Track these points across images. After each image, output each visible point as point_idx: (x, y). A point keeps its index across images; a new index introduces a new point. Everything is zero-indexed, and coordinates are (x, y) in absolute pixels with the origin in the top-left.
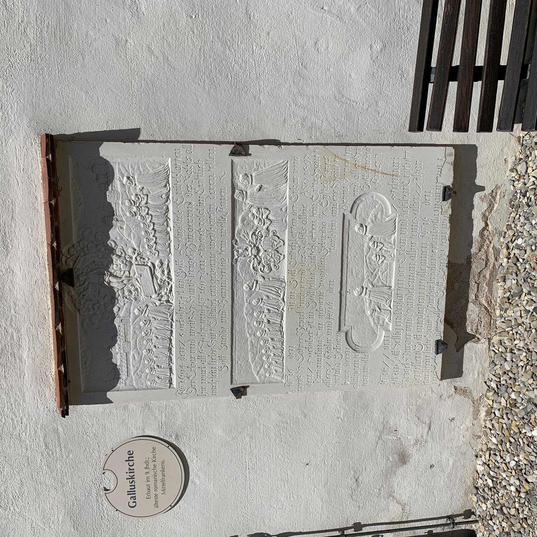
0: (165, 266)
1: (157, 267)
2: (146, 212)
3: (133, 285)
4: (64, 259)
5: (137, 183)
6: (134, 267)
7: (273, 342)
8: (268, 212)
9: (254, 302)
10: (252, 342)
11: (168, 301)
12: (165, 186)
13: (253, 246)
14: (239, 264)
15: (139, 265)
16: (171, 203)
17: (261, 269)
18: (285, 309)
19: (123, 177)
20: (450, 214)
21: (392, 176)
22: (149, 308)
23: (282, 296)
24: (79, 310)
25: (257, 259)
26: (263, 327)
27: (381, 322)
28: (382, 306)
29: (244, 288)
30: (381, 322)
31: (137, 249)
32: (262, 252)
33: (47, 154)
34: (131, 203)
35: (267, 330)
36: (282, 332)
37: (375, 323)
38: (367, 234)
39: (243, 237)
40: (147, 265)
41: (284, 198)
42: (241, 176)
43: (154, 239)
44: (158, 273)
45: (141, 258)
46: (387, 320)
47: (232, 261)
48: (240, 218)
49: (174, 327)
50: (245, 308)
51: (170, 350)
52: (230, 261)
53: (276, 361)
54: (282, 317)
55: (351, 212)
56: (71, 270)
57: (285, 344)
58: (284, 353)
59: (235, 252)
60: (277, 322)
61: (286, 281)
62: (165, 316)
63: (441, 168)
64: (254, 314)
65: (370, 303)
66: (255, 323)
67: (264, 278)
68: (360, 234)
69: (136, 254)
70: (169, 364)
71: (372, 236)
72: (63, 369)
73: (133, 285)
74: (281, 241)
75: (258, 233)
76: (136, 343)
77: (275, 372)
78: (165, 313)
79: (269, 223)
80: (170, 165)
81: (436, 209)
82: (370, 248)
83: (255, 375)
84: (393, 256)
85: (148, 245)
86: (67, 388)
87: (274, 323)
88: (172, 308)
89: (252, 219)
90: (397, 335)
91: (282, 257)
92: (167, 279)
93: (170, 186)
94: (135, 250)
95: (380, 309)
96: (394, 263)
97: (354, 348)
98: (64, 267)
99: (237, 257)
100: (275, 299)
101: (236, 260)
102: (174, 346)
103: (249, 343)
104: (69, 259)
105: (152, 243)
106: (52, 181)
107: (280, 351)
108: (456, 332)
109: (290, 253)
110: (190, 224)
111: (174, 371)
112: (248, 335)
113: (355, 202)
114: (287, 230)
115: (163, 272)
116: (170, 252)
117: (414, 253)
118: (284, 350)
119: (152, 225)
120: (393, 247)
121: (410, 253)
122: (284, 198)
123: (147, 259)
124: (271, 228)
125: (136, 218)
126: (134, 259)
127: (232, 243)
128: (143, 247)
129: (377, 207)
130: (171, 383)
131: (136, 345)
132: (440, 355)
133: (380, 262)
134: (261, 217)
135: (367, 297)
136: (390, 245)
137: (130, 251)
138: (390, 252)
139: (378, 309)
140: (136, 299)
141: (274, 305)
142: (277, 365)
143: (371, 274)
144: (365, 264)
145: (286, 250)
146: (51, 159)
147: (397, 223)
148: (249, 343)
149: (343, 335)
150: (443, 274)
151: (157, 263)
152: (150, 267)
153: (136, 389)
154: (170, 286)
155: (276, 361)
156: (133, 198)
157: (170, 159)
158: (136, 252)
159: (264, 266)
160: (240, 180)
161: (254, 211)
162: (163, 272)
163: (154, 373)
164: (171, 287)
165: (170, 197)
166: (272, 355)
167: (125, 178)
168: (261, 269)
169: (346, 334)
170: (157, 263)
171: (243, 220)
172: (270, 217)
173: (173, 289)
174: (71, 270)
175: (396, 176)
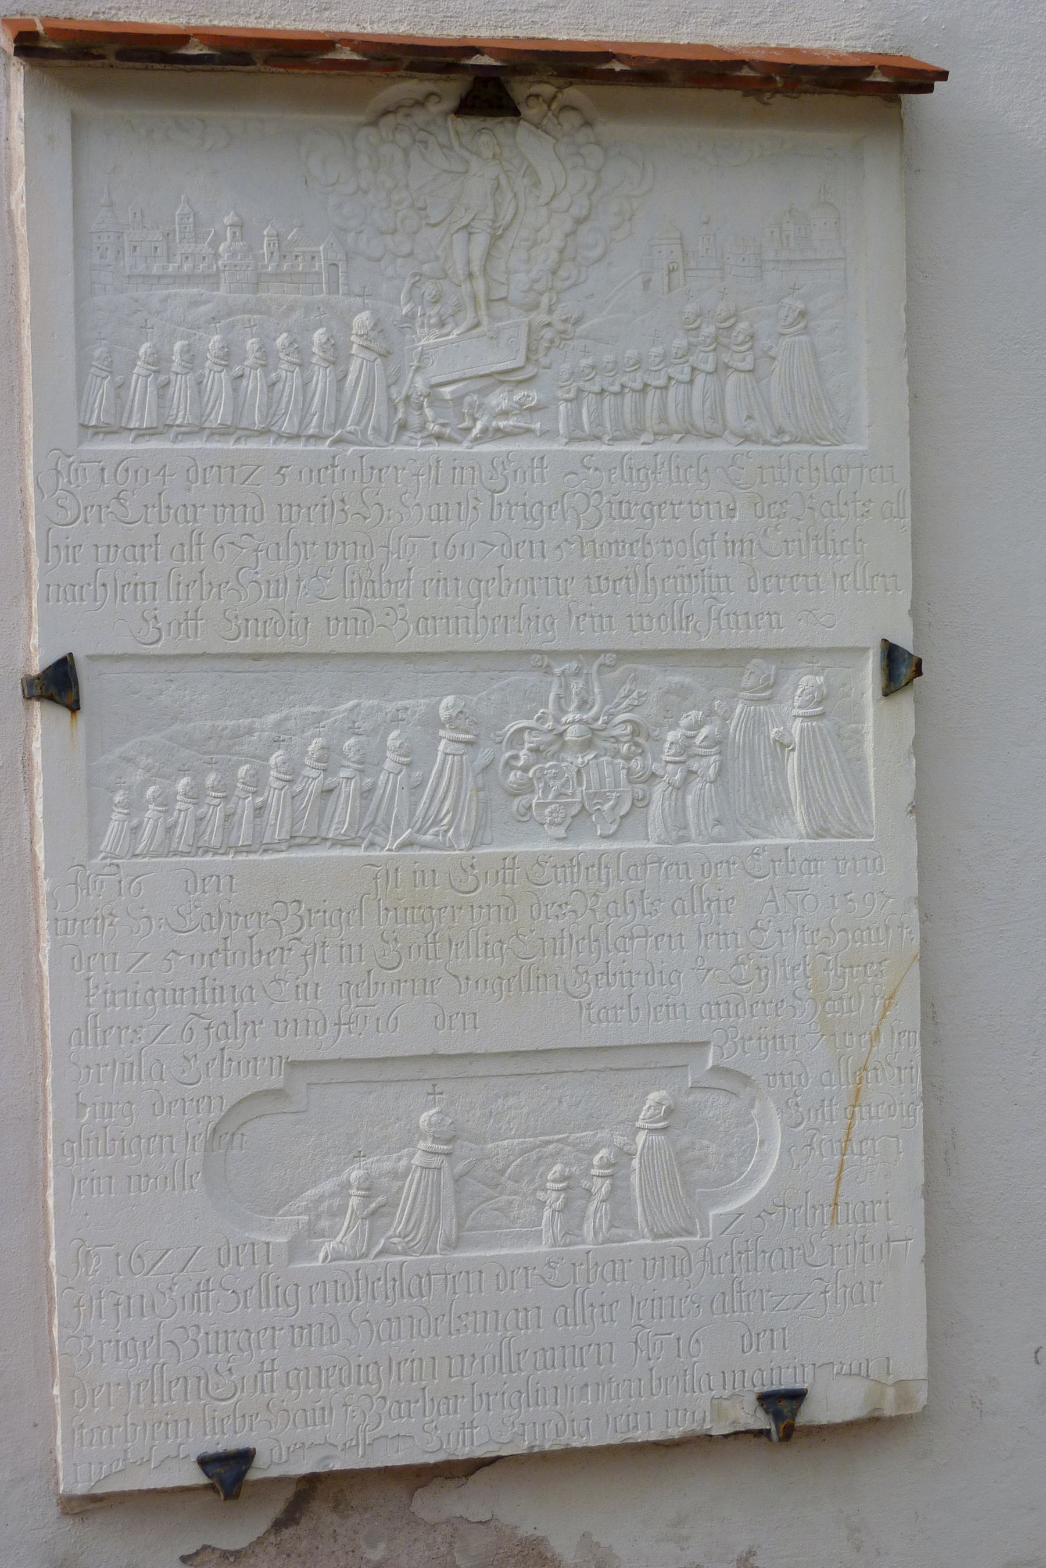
2: (702, 366)
4: (547, 90)
10: (250, 731)
11: (403, 427)
12: (781, 432)
13: (596, 726)
15: (530, 332)
16: (731, 448)
18: (375, 853)
24: (374, 123)
25: (551, 744)
28: (385, 1220)
31: (580, 329)
33: (885, 69)
34: (727, 319)
35: (297, 788)
36: (292, 842)
37: (321, 1199)
39: (623, 692)
40: (528, 359)
41: (754, 831)
42: (820, 680)
43: (616, 388)
44: (499, 399)
45: (552, 341)
47: (541, 652)
48: (687, 680)
52: (545, 647)
54: (343, 844)
56: (516, 113)
57: (241, 858)
58: (208, 858)
59: (574, 665)
60: (324, 826)
61: (474, 852)
63: (863, 1372)
67: (486, 768)
68: (639, 1111)
69: (560, 327)
70: (170, 426)
72: (195, 52)
73: (459, 308)
74: (614, 827)
76: (251, 312)
81: (729, 1377)
82: (593, 1151)
86: (113, 60)
94: (577, 322)
95: (373, 1213)
98: (519, 89)
100: (412, 814)
101: (548, 670)
102: (242, 446)
104: (545, 107)
106: (804, 78)
108: (260, 1541)
110: (666, 510)
112: (272, 718)
115: (505, 414)
117: (579, 1320)
118: (218, 858)
120: (600, 1237)
121: (578, 1305)
122: (754, 831)
123: (545, 361)
126: (544, 318)
127: (606, 652)
132: (199, 1478)
141: (389, 813)
142: (160, 831)
143: (500, 1166)
146: (871, 79)
147: (678, 1239)
149: (276, 1081)
150: (505, 1438)
152: (522, 368)
154: (456, 436)
156: (742, 326)
157: (865, 448)
159: (525, 769)
162: (505, 414)
164: (451, 440)
165: (746, 447)
167: (800, 305)
171: (683, 692)
174: (516, 113)
175: (834, 1215)
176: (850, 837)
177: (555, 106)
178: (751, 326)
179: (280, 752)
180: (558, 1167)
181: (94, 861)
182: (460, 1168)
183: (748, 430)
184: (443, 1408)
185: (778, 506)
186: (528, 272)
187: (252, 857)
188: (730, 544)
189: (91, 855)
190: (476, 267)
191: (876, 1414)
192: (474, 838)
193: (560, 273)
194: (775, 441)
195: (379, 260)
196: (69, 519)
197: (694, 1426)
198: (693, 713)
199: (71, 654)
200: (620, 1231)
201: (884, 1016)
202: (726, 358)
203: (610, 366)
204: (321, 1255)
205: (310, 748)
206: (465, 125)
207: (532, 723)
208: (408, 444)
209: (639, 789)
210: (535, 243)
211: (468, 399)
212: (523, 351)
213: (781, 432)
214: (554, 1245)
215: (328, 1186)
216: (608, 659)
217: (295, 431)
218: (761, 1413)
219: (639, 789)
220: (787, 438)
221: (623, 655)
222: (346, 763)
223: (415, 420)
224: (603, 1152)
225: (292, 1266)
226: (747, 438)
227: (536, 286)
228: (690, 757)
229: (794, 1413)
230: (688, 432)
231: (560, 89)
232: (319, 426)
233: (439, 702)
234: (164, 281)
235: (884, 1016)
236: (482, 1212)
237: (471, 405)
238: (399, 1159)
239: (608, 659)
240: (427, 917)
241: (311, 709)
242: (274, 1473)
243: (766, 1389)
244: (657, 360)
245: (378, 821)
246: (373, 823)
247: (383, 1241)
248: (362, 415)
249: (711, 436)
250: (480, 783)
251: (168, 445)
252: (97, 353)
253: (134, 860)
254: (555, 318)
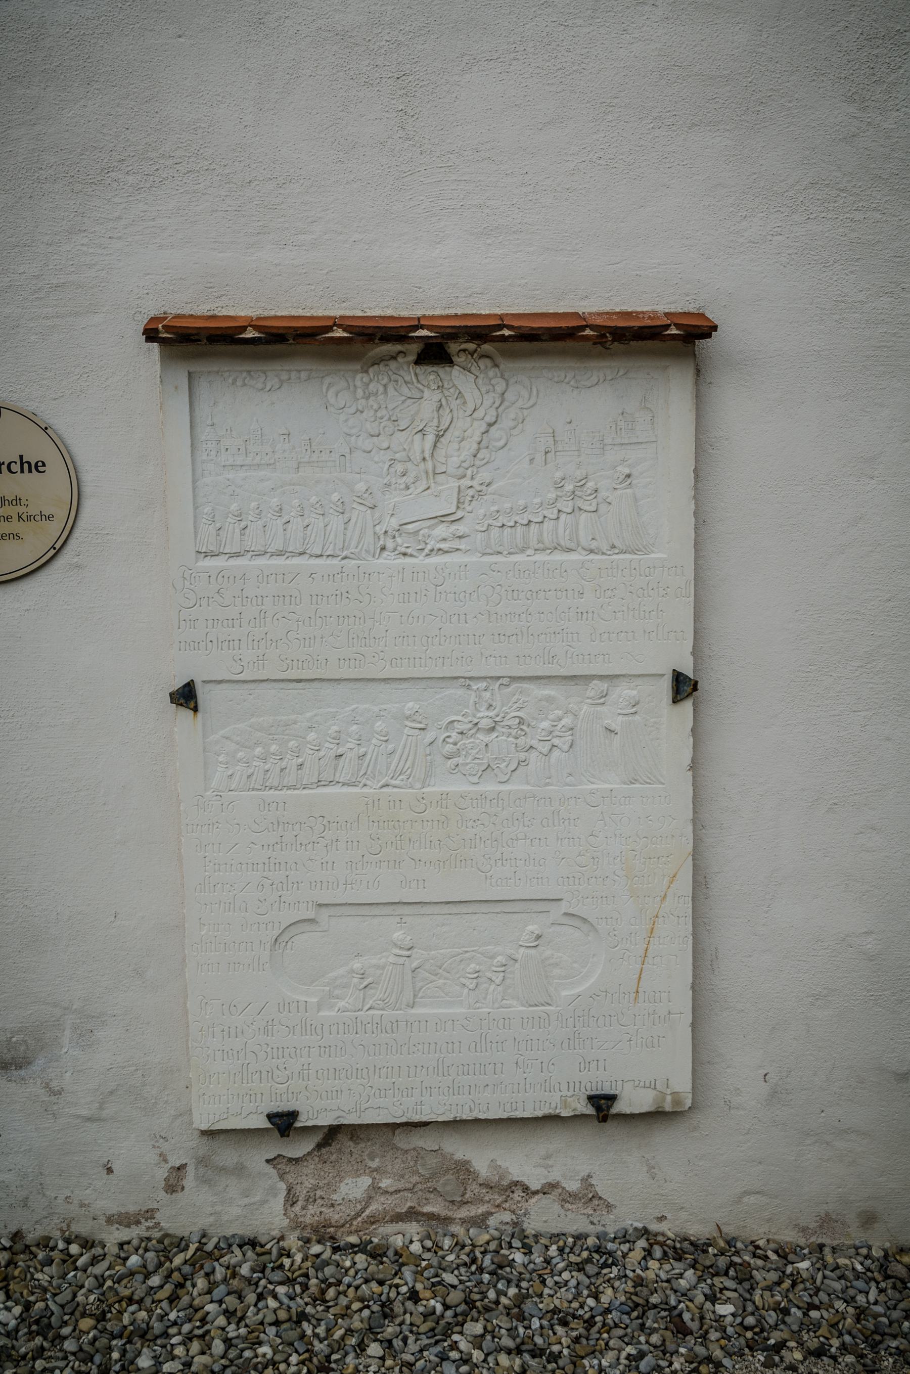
0: (456, 544)
1: (454, 527)
2: (564, 509)
3: (417, 479)
5: (619, 492)
6: (454, 484)
7: (294, 768)
8: (566, 747)
9: (379, 725)
10: (295, 723)
11: (383, 549)
13: (497, 719)
14: (461, 692)
15: (459, 491)
16: (581, 557)
17: (449, 737)
18: (365, 790)
19: (629, 466)
20: (562, 1115)
21: (635, 990)
22: (369, 511)
23: (393, 782)
26: (327, 745)
27: (337, 992)
28: (373, 991)
29: (410, 704)
30: (337, 992)
31: (491, 489)
32: (486, 738)
34: (581, 481)
35: (322, 753)
36: (319, 783)
38: (522, 950)
39: (514, 699)
40: (458, 507)
41: (592, 780)
42: (635, 692)
43: (512, 524)
44: (441, 530)
45: (473, 497)
46: (342, 1004)
48: (553, 693)
49: (330, 561)
50: (367, 706)
51: (280, 554)
52: (466, 675)
53: (252, 774)
54: (348, 785)
55: (566, 914)
57: (289, 792)
58: (272, 792)
59: (485, 684)
60: (337, 775)
61: (424, 790)
62: (354, 543)
64: (355, 727)
65: (377, 967)
66: (335, 728)
69: (479, 488)
71: (516, 961)
73: (417, 479)
74: (507, 777)
75: (522, 730)
76: (294, 484)
77: (230, 773)
78: (359, 543)
79: (545, 750)
80: (653, 555)
81: (572, 1085)
82: (492, 957)
83: (221, 733)
84: (478, 1005)
85: (498, 512)
87: (335, 769)
88: (370, 558)
89: (551, 717)
90: (309, 1027)
91: (475, 779)
92: (429, 547)
93: (615, 557)
96: (464, 1010)
97: (280, 940)
98: (453, 347)
99: (475, 688)
100: (388, 768)
101: (469, 687)
102: (288, 562)
103: (293, 717)
105: (502, 520)
107: (275, 784)
108: (309, 1154)
109: (483, 796)
111: (233, 562)
112: (309, 715)
113: (585, 920)
114: (529, 788)
116: (484, 554)
117: (484, 1050)
118: (277, 792)
119: (540, 519)
120: (496, 1005)
121: (483, 1042)
123: (469, 508)
124: (533, 755)
125: (552, 489)
126: (470, 483)
128: (493, 503)
129: (575, 965)
130: (206, 555)
131: (290, 484)
132: (267, 1125)
133: (463, 980)
134: (554, 734)
135: (392, 959)
136: (500, 998)
137: (484, 475)
138: (485, 998)
139: (365, 983)
140: (388, 485)
142: (245, 777)
144: (460, 951)
145: (489, 787)
148: (293, 717)
149: (310, 914)
151: (461, 528)
153: (194, 481)
154: (415, 554)
155: (252, 774)
156: (590, 484)
157: (665, 556)
158: (484, 488)
159: (455, 744)
161: (567, 721)
163: (229, 520)
165: (592, 556)
166: (267, 767)
167: (627, 471)
168: (449, 737)
169: (311, 921)
170: (461, 528)
171: (549, 699)
172: (556, 753)
173: (408, 560)
177: (475, 355)
178: (596, 484)
179: (313, 734)
180: (473, 966)
181: (208, 793)
182: (414, 965)
183: (592, 547)
184: (405, 1094)
185: (609, 592)
186: (459, 456)
187: (296, 792)
188: (580, 614)
189: (206, 791)
190: (427, 455)
191: (660, 1110)
192: (424, 782)
193: (478, 456)
194: (609, 553)
195: (370, 452)
196: (191, 605)
197: (550, 1111)
198: (556, 712)
199: (192, 681)
200: (508, 1002)
201: (669, 887)
202: (579, 503)
203: (508, 511)
204: (336, 1009)
205: (330, 732)
206: (419, 370)
207: (459, 718)
208: (386, 559)
209: (522, 756)
210: (463, 439)
211: (422, 532)
212: (455, 503)
213: (613, 547)
214: (469, 1008)
215: (341, 971)
216: (505, 681)
217: (319, 553)
218: (589, 1106)
219: (522, 756)
220: (617, 551)
221: (514, 679)
222: (350, 740)
223: (390, 544)
224: (499, 958)
225: (320, 1014)
226: (592, 551)
227: (464, 465)
228: (553, 737)
229: (609, 1107)
230: (556, 548)
231: (479, 345)
232: (334, 550)
233: (404, 706)
234: (244, 468)
235: (669, 887)
236: (428, 988)
237: (424, 536)
238: (380, 959)
239: (505, 681)
240: (396, 826)
241: (332, 710)
242: (310, 1123)
243: (593, 1093)
244: (537, 506)
245: (369, 772)
246: (365, 774)
247: (371, 1002)
248: (359, 543)
249: (570, 550)
250: (428, 752)
251: (248, 563)
252: (205, 511)
253: (230, 793)
254: (475, 483)
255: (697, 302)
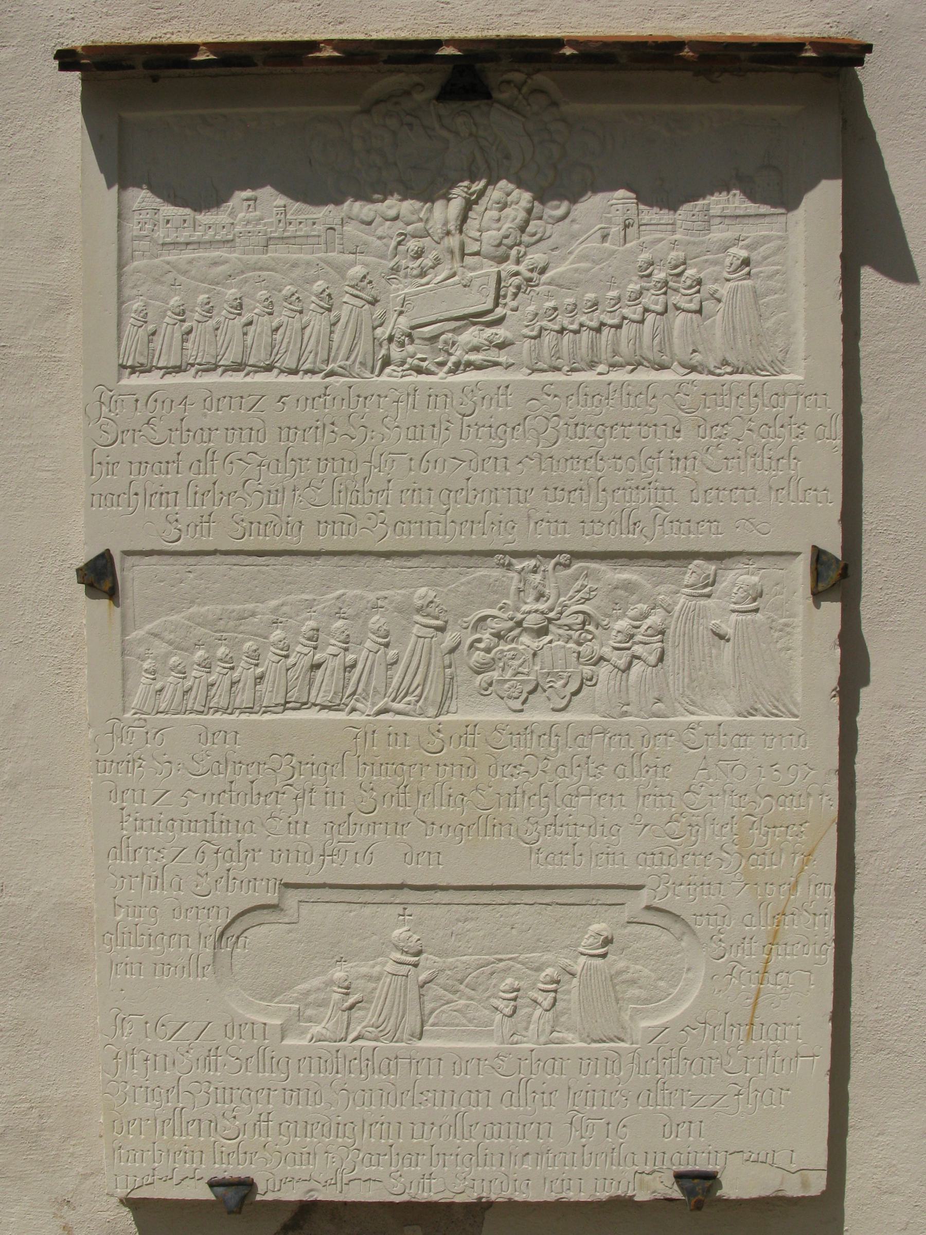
0: (493, 355)
1: (489, 331)
2: (653, 307)
3: (437, 262)
4: (518, 77)
5: (731, 284)
6: (491, 269)
7: (251, 682)
8: (653, 659)
9: (375, 620)
10: (253, 614)
11: (387, 362)
12: (725, 363)
13: (551, 615)
14: (497, 573)
17: (479, 640)
18: (355, 716)
19: (747, 247)
20: (636, 1199)
21: (748, 1021)
22: (367, 306)
23: (395, 705)
24: (367, 111)
25: (511, 630)
26: (299, 648)
27: (309, 1012)
28: (361, 1013)
29: (423, 591)
30: (309, 1012)
32: (535, 644)
34: (676, 267)
35: (291, 661)
36: (285, 706)
37: (308, 993)
38: (583, 959)
39: (577, 586)
40: (497, 304)
41: (692, 708)
42: (755, 579)
43: (575, 327)
45: (519, 288)
46: (316, 1029)
47: (504, 553)
49: (307, 378)
50: (358, 592)
51: (238, 367)
52: (507, 547)
53: (191, 689)
54: (329, 708)
55: (648, 908)
56: (488, 96)
57: (244, 717)
58: (218, 716)
59: (533, 562)
60: (314, 693)
61: (441, 718)
62: (343, 352)
63: (769, 1160)
64: (340, 623)
65: (369, 978)
66: (312, 624)
67: (452, 651)
68: (582, 938)
69: (529, 275)
70: (193, 365)
71: (573, 975)
73: (437, 262)
74: (565, 702)
75: (589, 632)
76: (261, 269)
77: (158, 686)
78: (351, 351)
79: (622, 663)
80: (783, 377)
81: (651, 1156)
82: (539, 969)
83: (148, 627)
84: (516, 1038)
85: (555, 309)
87: (311, 685)
88: (368, 374)
89: (631, 613)
90: (268, 1061)
91: (517, 705)
92: (453, 359)
93: (727, 377)
94: (543, 271)
95: (351, 1007)
96: (495, 1045)
97: (228, 933)
99: (519, 567)
100: (387, 686)
101: (509, 566)
102: (248, 379)
103: (250, 606)
104: (515, 91)
105: (563, 320)
107: (223, 703)
109: (527, 728)
110: (619, 428)
111: (170, 380)
112: (273, 603)
113: (677, 917)
114: (597, 718)
115: (476, 349)
116: (534, 371)
117: (522, 1102)
118: (225, 716)
119: (616, 321)
120: (543, 1039)
122: (692, 708)
123: (514, 304)
124: (604, 670)
125: (635, 278)
126: (515, 268)
127: (561, 552)
128: (549, 296)
129: (661, 984)
130: (133, 370)
131: (255, 270)
133: (496, 1002)
134: (636, 639)
135: (390, 967)
136: (548, 1028)
137: (536, 257)
138: (526, 1029)
139: (351, 1000)
140: (395, 270)
141: (368, 683)
142: (179, 694)
143: (459, 976)
144: (491, 958)
145: (538, 715)
147: (612, 1044)
148: (250, 606)
149: (271, 898)
150: (456, 1189)
151: (501, 332)
152: (490, 311)
153: (120, 266)
154: (433, 369)
155: (191, 689)
156: (690, 272)
157: (801, 378)
158: (535, 275)
159: (488, 650)
160: (738, 578)
161: (654, 619)
162: (476, 349)
163: (167, 320)
164: (429, 372)
165: (694, 376)
166: (212, 678)
167: (744, 254)
168: (479, 640)
169: (273, 907)
170: (501, 332)
171: (629, 587)
172: (637, 667)
173: (423, 378)
174: (488, 96)
175: (749, 1034)
176: (777, 716)
177: (525, 90)
178: (699, 272)
179: (278, 632)
180: (509, 981)
181: (128, 715)
182: (423, 977)
183: (694, 362)
184: (407, 1162)
185: (719, 428)
186: (499, 229)
187: (253, 717)
188: (674, 461)
189: (124, 711)
190: (452, 227)
191: (780, 1194)
192: (441, 707)
193: (528, 229)
194: (718, 371)
195: (369, 223)
196: (109, 442)
197: (619, 1192)
198: (639, 606)
199: (108, 550)
200: (560, 1035)
201: (802, 870)
202: (675, 299)
203: (570, 308)
204: (309, 1036)
205: (304, 628)
206: (444, 109)
207: (494, 612)
208: (390, 376)
209: (587, 670)
210: (505, 206)
211: (443, 337)
212: (492, 295)
213: (725, 363)
214: (503, 1043)
215: (316, 982)
216: (562, 559)
217: (294, 366)
218: (676, 1187)
219: (587, 670)
220: (729, 369)
221: (577, 555)
222: (333, 641)
223: (396, 353)
224: (549, 971)
225: (286, 1042)
226: (693, 369)
227: (505, 241)
228: (634, 643)
230: (640, 364)
231: (529, 75)
232: (315, 363)
233: (413, 593)
234: (190, 247)
235: (802, 870)
236: (443, 1012)
237: (446, 342)
238: (373, 966)
239: (562, 559)
240: (399, 771)
241: (305, 596)
242: (269, 1197)
243: (682, 1168)
244: (613, 302)
245: (359, 691)
246: (354, 693)
247: (359, 1028)
248: (351, 351)
249: (662, 367)
250: (447, 662)
251: (191, 380)
252: (135, 307)
253: (159, 716)
254: (522, 268)
255: (841, 26)
